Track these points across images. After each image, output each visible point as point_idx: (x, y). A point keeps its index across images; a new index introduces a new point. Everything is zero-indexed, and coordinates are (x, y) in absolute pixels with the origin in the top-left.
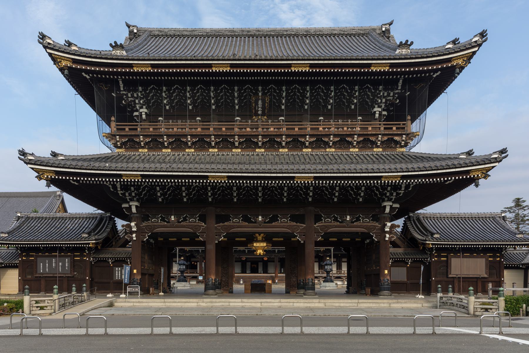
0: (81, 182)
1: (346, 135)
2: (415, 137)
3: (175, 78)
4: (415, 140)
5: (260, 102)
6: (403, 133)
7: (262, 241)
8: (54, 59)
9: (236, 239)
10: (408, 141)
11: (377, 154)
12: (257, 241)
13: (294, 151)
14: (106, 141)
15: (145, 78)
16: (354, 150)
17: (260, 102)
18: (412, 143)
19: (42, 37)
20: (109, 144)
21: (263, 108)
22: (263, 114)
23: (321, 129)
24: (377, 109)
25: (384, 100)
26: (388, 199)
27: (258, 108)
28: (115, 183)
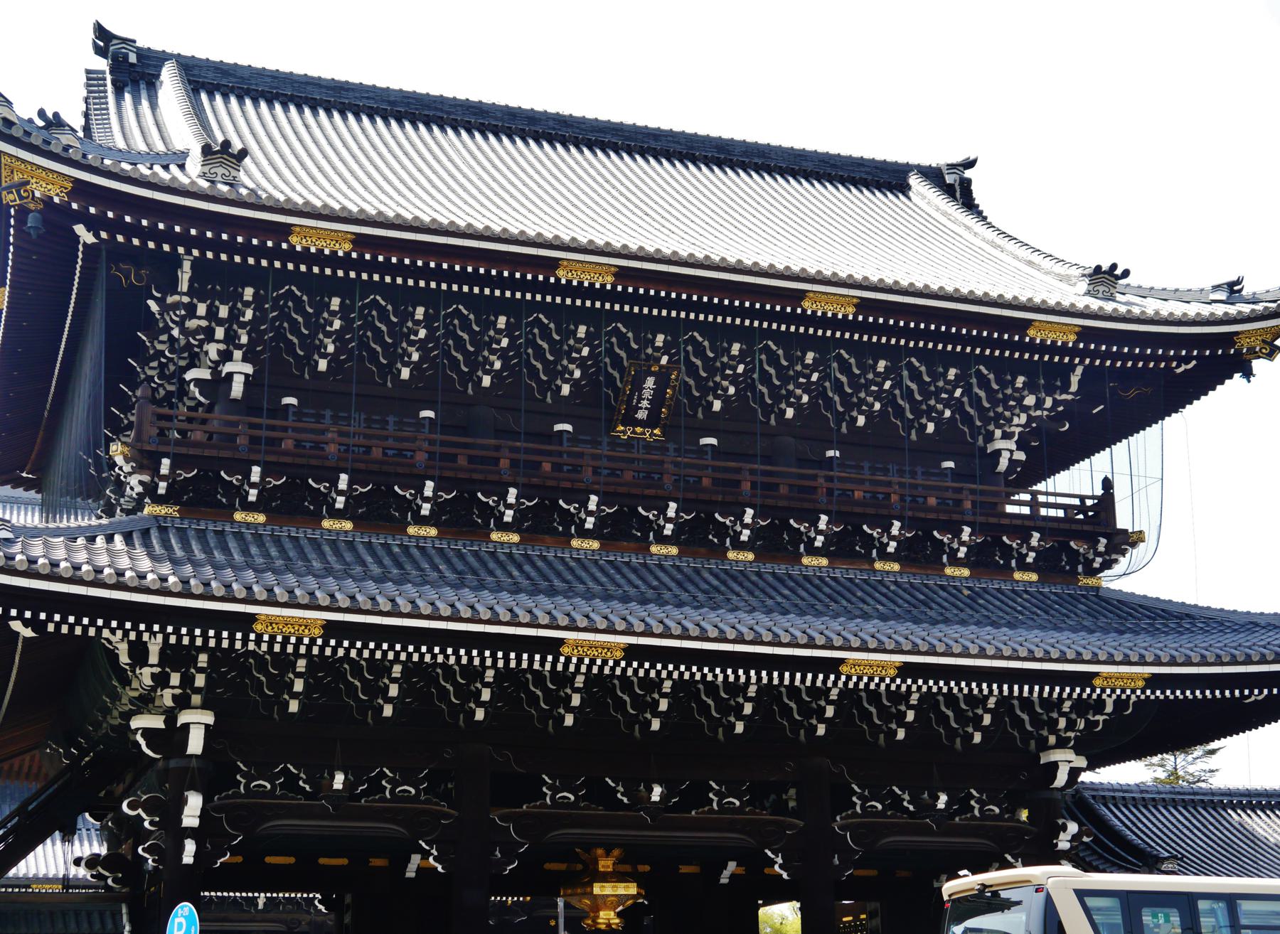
0: (51, 628)
1: (938, 520)
2: (1134, 545)
5: (650, 382)
6: (1098, 529)
7: (617, 876)
9: (547, 866)
10: (1114, 556)
11: (896, 583)
12: (605, 878)
13: (773, 559)
16: (741, 557)
17: (650, 382)
18: (1123, 564)
22: (651, 422)
23: (858, 495)
26: (1059, 738)
27: (640, 399)
28: (146, 637)
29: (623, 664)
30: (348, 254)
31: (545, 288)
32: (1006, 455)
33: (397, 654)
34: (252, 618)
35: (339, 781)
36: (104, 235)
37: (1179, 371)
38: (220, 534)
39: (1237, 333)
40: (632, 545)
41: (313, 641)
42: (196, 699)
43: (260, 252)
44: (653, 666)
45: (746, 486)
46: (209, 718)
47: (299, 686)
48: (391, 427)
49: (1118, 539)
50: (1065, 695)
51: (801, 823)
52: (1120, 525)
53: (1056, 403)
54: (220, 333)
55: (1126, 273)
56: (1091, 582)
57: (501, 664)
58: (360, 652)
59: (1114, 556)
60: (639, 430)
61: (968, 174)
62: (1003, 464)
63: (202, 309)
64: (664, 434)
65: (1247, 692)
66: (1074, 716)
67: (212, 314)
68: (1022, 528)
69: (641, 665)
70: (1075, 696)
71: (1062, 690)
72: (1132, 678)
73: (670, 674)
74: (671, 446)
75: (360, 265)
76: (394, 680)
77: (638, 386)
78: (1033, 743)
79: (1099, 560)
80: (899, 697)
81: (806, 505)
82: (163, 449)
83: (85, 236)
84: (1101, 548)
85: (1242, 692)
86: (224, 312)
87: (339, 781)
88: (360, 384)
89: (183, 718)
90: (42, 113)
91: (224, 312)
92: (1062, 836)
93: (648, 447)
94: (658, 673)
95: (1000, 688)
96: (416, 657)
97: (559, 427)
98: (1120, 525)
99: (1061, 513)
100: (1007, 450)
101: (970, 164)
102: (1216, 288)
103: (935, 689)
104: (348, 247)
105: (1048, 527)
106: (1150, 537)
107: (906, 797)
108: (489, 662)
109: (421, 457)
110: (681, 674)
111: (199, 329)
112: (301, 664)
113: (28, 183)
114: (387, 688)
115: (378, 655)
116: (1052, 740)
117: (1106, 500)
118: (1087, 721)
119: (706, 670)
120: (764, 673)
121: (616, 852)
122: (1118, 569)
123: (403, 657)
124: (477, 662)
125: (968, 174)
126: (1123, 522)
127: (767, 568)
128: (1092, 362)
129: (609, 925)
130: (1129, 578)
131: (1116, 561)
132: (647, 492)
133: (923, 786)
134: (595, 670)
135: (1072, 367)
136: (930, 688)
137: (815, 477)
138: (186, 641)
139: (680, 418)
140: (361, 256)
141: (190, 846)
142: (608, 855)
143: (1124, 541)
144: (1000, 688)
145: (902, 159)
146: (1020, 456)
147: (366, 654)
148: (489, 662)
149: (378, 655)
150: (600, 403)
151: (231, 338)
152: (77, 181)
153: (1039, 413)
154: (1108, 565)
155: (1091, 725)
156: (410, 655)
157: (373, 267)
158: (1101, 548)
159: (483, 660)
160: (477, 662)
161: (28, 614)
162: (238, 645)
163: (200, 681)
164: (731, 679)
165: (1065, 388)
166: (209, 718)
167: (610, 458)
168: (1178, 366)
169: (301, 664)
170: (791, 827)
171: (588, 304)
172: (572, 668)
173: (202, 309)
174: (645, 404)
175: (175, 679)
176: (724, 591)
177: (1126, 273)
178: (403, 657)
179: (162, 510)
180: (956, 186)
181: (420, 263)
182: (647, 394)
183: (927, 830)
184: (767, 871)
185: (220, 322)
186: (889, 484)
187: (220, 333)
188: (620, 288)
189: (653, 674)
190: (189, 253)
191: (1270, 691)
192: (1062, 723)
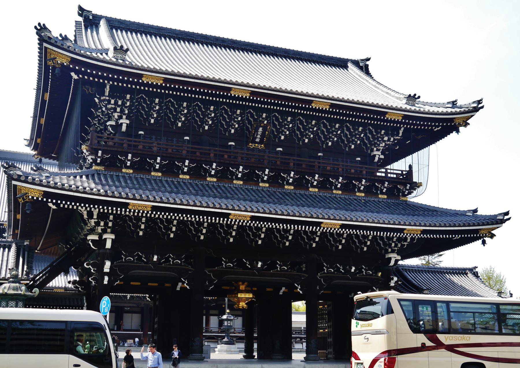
0: (62, 206)
2: (418, 187)
3: (209, 98)
5: (261, 129)
7: (246, 291)
9: (223, 287)
10: (412, 191)
11: (340, 197)
12: (242, 292)
13: (300, 189)
15: (159, 91)
17: (261, 129)
18: (415, 192)
21: (263, 135)
22: (261, 142)
26: (392, 250)
27: (257, 135)
28: (93, 209)
29: (250, 222)
30: (161, 84)
31: (227, 97)
32: (377, 156)
33: (175, 217)
34: (128, 204)
35: (155, 258)
36: (81, 76)
37: (435, 130)
38: (118, 176)
39: (455, 118)
40: (254, 183)
41: (148, 212)
42: (109, 230)
43: (132, 83)
44: (260, 223)
45: (292, 164)
46: (113, 237)
47: (143, 227)
48: (175, 142)
49: (413, 185)
50: (394, 236)
51: (307, 276)
52: (414, 181)
53: (394, 140)
54: (118, 109)
55: (419, 97)
56: (404, 199)
57: (209, 221)
58: (163, 216)
59: (412, 191)
60: (256, 145)
61: (367, 63)
62: (376, 159)
63: (113, 102)
64: (265, 146)
65: (454, 236)
66: (397, 243)
67: (116, 103)
68: (382, 180)
69: (256, 223)
70: (398, 236)
71: (394, 234)
72: (417, 230)
73: (265, 226)
74: (267, 151)
75: (165, 88)
76: (174, 226)
77: (257, 131)
78: (383, 251)
79: (407, 192)
80: (340, 235)
81: (311, 171)
82: (99, 147)
83: (75, 77)
84: (408, 188)
85: (452, 236)
86: (120, 103)
87: (155, 258)
88: (165, 128)
89: (105, 236)
90: (61, 35)
91: (120, 103)
92: (392, 281)
93: (259, 151)
94: (261, 225)
95: (373, 233)
96: (181, 218)
97: (230, 143)
98: (414, 181)
99: (395, 176)
100: (378, 155)
101: (368, 59)
102: (448, 103)
103: (352, 233)
104: (161, 82)
105: (391, 181)
106: (424, 185)
107: (341, 268)
108: (205, 220)
109: (184, 152)
110: (269, 226)
111: (112, 108)
112: (144, 220)
113: (56, 58)
114: (172, 228)
115: (169, 217)
116: (390, 250)
117: (410, 172)
118: (401, 244)
119: (277, 225)
120: (296, 226)
121: (246, 283)
122: (413, 195)
123: (177, 218)
124: (202, 220)
125: (367, 63)
126: (415, 179)
127: (298, 192)
128: (407, 126)
129: (243, 307)
130: (417, 198)
131: (413, 192)
132: (259, 165)
133: (347, 265)
134: (240, 224)
135: (400, 128)
136: (350, 232)
137: (314, 162)
138: (106, 211)
139: (270, 141)
140: (166, 85)
141: (106, 278)
142: (243, 284)
143: (415, 186)
144: (373, 233)
145: (346, 57)
146: (382, 157)
147: (165, 217)
148: (205, 220)
149: (169, 217)
150: (244, 136)
151: (122, 111)
152: (72, 58)
153: (389, 143)
154: (410, 193)
155: (402, 245)
156: (180, 217)
157: (169, 89)
158: (408, 188)
159: (204, 219)
160: (202, 220)
161: (54, 201)
162: (123, 213)
163: (110, 224)
164: (285, 228)
165: (398, 135)
166: (113, 237)
167: (247, 154)
168: (435, 128)
169: (144, 220)
170: (304, 276)
171: (241, 103)
172: (233, 223)
173: (113, 102)
174: (259, 136)
175: (102, 223)
176: (284, 199)
177: (419, 97)
178: (177, 218)
179: (98, 168)
180: (363, 66)
181: (185, 88)
182: (260, 133)
183: (348, 279)
184: (295, 291)
185: (119, 106)
186: (339, 165)
187: (118, 109)
188: (251, 98)
189: (259, 225)
190: (109, 82)
191: (461, 236)
192: (393, 245)
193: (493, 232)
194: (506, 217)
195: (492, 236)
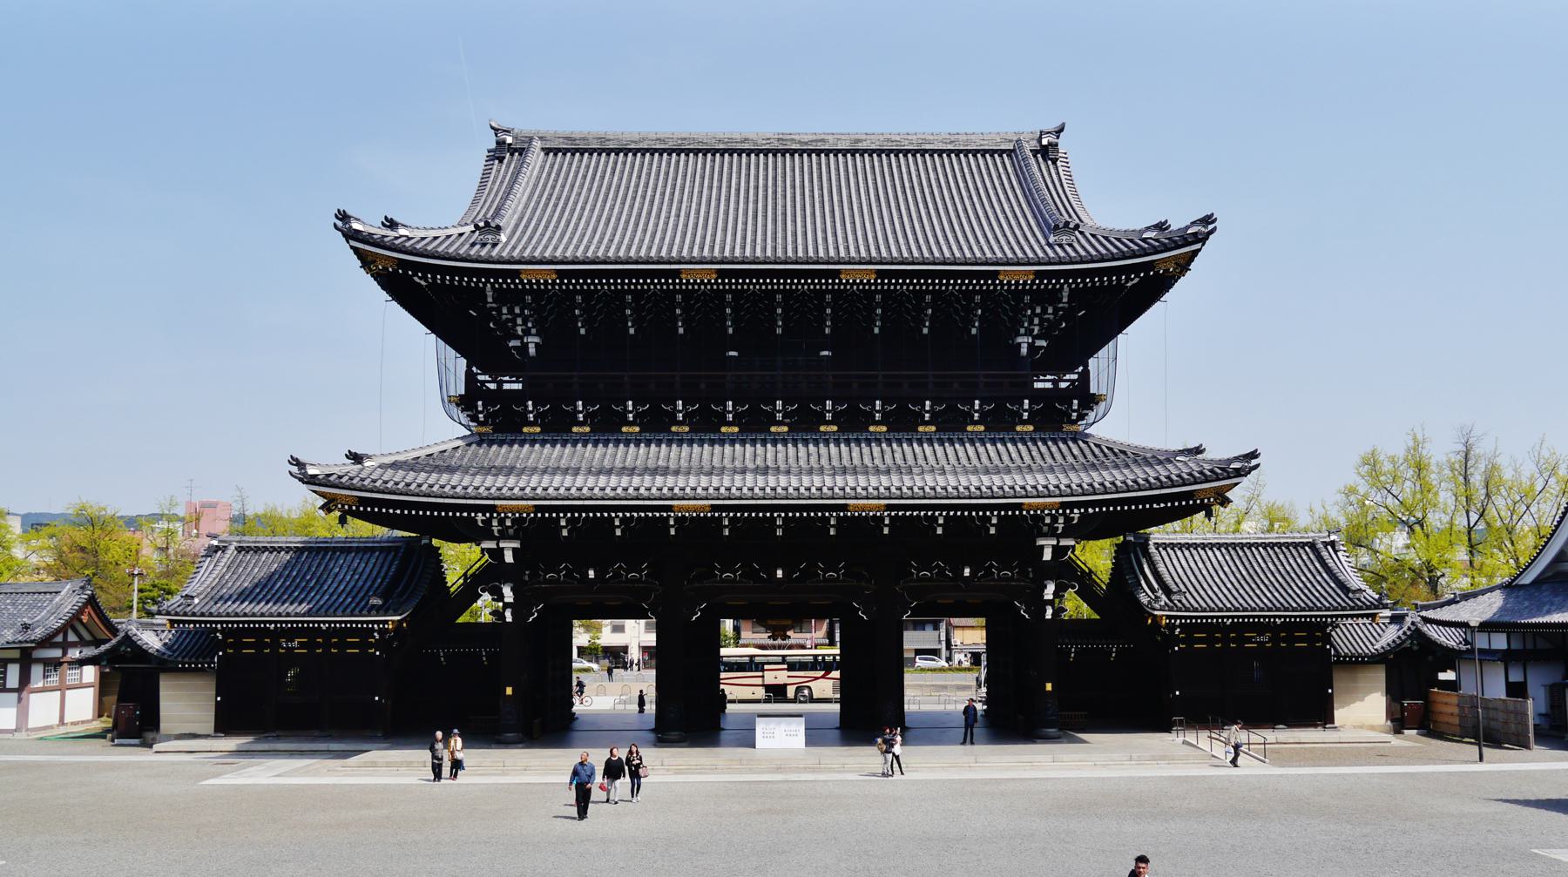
4: (1102, 405)
8: (366, 261)
14: (455, 411)
18: (1091, 416)
19: (344, 217)
20: (463, 418)
24: (1024, 342)
25: (1036, 321)
46: (516, 545)
54: (519, 321)
56: (1073, 428)
62: (1024, 351)
63: (505, 310)
67: (511, 311)
86: (517, 310)
91: (517, 310)
101: (1060, 130)
154: (1081, 417)
155: (1068, 520)
163: (508, 523)
166: (516, 545)
173: (505, 310)
187: (519, 321)
192: (1048, 520)
193: (1228, 494)
194: (1254, 462)
195: (1225, 502)
